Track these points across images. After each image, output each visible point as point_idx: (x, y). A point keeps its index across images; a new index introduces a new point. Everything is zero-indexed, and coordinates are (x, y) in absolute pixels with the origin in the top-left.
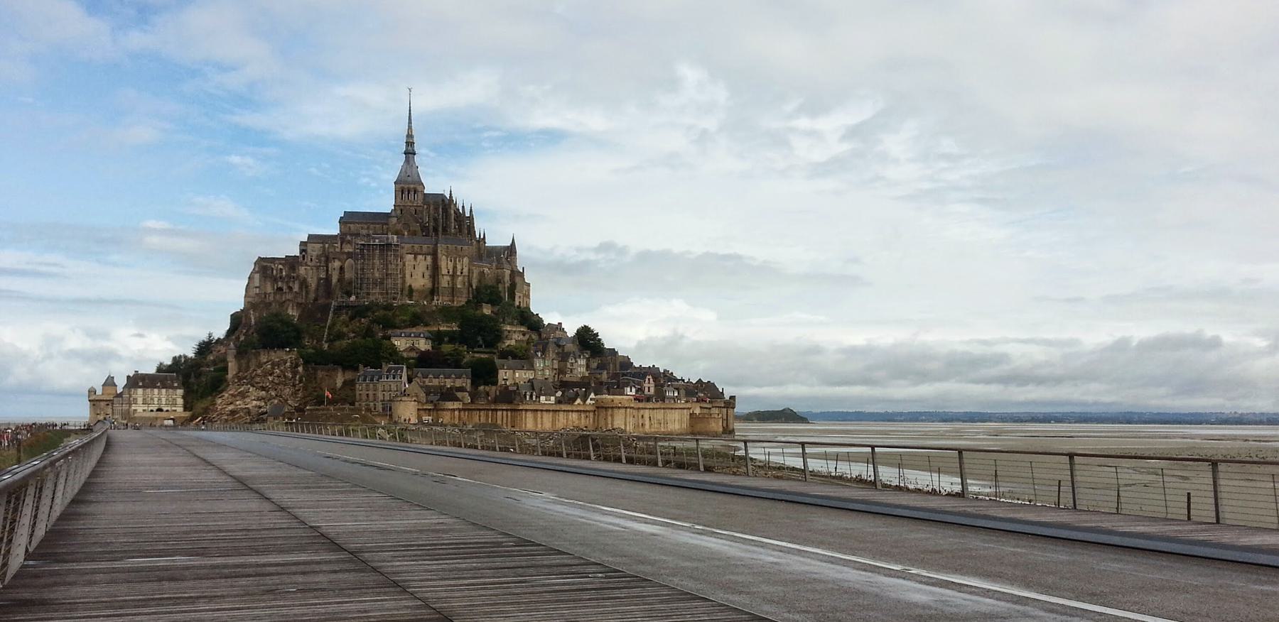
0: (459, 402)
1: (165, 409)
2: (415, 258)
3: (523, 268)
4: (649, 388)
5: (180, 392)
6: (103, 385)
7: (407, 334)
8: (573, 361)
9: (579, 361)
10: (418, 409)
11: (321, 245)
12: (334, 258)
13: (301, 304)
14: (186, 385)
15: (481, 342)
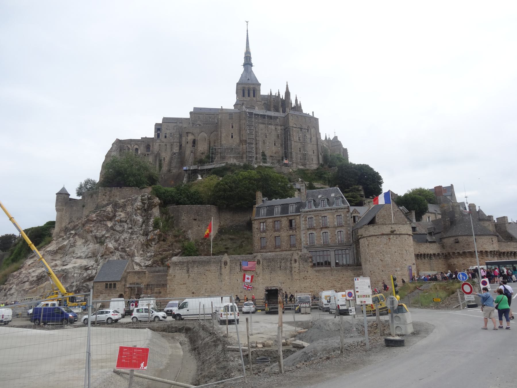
11: (175, 124)
12: (187, 133)
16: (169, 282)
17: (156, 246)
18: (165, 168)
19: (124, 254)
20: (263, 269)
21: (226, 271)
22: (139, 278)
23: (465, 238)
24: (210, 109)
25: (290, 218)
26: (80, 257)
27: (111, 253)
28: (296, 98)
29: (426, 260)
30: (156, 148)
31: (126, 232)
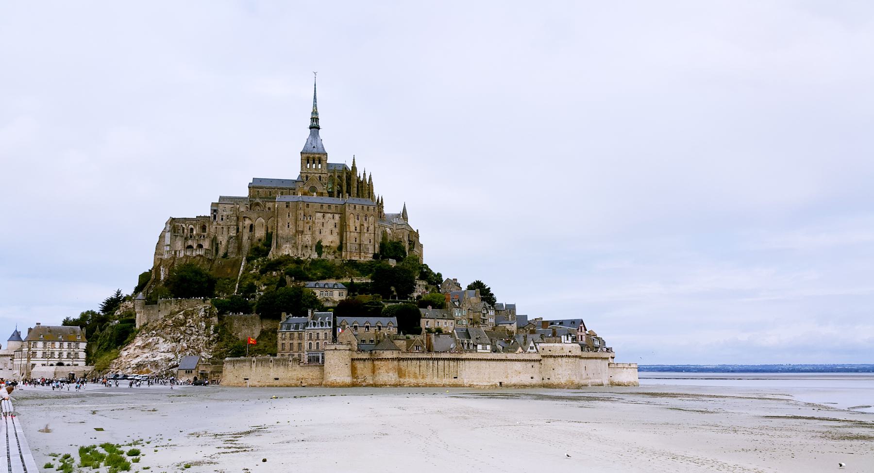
0: (398, 351)
1: (66, 363)
2: (324, 216)
3: (417, 230)
4: (582, 336)
5: (83, 346)
6: (8, 341)
7: (322, 286)
8: (485, 312)
9: (490, 312)
10: (353, 360)
11: (232, 206)
12: (244, 217)
13: (211, 260)
14: (90, 337)
15: (395, 294)
16: (223, 371)
17: (215, 345)
18: (221, 252)
19: (194, 350)
20: (273, 365)
21: (254, 365)
22: (206, 368)
23: (379, 351)
24: (272, 180)
25: (300, 332)
26: (164, 352)
27: (186, 350)
28: (365, 172)
29: (362, 362)
30: (211, 229)
31: (194, 334)
